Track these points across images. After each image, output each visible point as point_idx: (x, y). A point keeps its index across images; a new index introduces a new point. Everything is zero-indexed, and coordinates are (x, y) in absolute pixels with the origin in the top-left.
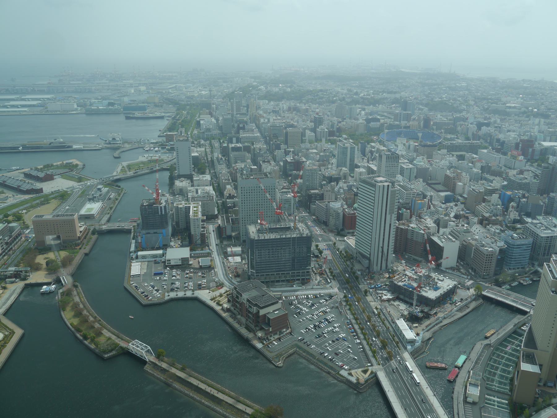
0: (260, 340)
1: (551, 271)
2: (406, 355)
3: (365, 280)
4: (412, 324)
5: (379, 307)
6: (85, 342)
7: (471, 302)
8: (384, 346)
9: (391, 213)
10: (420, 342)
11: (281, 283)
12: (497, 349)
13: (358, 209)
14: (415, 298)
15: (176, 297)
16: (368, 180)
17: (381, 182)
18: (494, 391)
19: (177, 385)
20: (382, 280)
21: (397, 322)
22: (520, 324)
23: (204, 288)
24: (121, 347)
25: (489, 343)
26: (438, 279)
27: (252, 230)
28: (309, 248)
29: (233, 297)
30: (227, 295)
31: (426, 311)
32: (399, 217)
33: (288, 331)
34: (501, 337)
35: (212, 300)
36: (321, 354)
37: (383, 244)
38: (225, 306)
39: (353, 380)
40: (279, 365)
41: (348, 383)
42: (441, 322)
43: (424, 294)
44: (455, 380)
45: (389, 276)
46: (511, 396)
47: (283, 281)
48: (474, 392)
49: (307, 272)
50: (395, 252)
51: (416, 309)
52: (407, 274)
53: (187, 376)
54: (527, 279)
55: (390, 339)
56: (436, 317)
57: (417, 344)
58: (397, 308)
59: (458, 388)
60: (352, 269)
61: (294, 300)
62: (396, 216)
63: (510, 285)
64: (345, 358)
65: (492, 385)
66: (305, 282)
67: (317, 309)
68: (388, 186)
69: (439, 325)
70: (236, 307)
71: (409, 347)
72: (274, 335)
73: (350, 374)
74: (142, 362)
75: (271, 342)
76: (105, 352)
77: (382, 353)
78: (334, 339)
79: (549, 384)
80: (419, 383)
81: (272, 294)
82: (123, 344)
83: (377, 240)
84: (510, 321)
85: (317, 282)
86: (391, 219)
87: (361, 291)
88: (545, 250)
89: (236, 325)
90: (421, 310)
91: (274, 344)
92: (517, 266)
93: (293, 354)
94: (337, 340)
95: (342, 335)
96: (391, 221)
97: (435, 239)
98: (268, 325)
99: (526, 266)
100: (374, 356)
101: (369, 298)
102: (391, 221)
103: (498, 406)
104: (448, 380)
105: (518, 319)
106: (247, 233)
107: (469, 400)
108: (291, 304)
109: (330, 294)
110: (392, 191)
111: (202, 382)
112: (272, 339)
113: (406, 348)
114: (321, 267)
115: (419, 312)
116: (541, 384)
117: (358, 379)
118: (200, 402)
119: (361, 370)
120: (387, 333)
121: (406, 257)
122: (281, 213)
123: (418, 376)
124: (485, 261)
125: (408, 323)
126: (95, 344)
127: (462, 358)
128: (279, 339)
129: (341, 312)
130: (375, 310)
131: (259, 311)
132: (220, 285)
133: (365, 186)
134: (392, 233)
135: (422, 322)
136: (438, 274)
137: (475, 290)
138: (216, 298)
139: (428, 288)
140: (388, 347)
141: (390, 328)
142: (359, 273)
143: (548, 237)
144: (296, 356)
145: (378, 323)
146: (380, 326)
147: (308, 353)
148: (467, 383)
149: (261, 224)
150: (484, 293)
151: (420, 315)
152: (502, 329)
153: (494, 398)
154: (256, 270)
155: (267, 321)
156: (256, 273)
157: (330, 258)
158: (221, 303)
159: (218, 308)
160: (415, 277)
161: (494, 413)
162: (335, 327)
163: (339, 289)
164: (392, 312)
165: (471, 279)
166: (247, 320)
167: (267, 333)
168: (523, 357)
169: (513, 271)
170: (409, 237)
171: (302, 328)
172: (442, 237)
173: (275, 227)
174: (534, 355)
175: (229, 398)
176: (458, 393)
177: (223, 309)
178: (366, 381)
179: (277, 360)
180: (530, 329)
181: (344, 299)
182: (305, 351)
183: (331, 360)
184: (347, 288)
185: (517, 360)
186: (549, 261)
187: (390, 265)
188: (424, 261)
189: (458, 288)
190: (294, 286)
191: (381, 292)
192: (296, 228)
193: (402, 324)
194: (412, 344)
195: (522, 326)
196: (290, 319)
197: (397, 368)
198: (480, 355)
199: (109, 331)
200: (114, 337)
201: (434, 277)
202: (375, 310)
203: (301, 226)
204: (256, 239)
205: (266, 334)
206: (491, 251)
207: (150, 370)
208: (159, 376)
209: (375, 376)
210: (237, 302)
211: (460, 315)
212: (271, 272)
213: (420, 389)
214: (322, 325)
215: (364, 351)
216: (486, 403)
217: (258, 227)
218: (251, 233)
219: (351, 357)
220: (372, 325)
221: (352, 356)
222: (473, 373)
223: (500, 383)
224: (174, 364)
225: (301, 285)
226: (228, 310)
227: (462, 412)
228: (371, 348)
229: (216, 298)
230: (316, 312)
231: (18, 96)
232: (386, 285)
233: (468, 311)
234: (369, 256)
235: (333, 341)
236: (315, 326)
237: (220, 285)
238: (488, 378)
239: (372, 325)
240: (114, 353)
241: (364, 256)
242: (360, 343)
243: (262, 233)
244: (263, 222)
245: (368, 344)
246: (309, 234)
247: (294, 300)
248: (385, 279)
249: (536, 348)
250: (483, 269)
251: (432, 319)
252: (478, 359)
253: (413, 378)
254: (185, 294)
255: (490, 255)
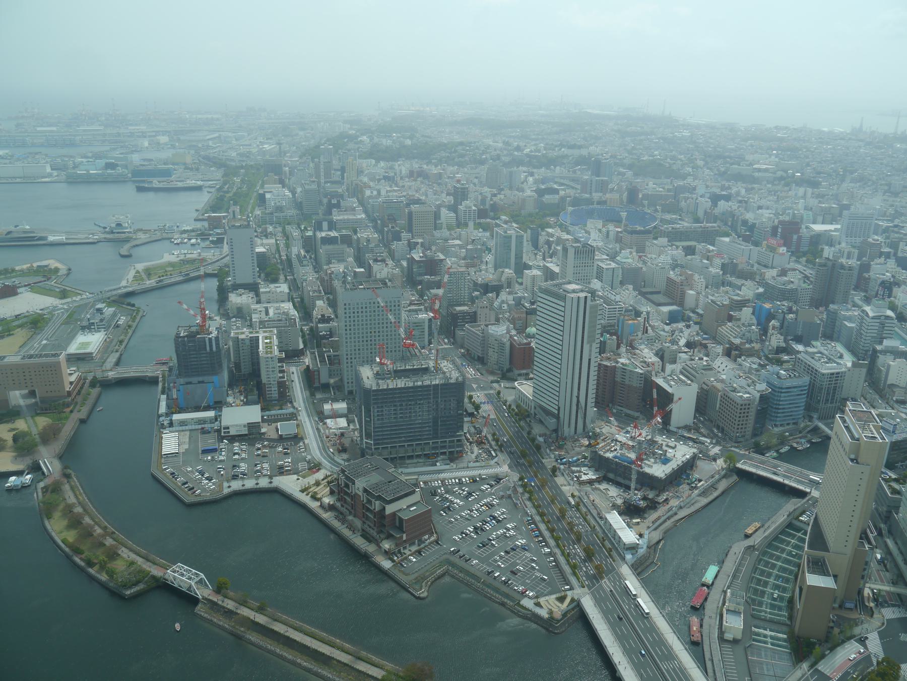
0: (388, 554)
1: (847, 428)
2: (625, 570)
3: (551, 450)
4: (631, 519)
5: (576, 493)
6: (90, 570)
7: (719, 480)
8: (589, 555)
9: (590, 342)
10: (645, 547)
11: (415, 461)
12: (764, 553)
13: (537, 336)
14: (634, 477)
15: (241, 488)
16: (552, 288)
17: (574, 291)
18: (765, 620)
19: (253, 637)
20: (577, 449)
21: (608, 516)
22: (797, 513)
23: (289, 473)
24: (154, 577)
25: (752, 544)
26: (667, 446)
27: (367, 374)
28: (460, 402)
29: (338, 485)
30: (329, 483)
31: (650, 496)
32: (602, 349)
33: (432, 539)
34: (770, 534)
35: (302, 491)
36: (489, 573)
37: (579, 394)
38: (327, 500)
39: (544, 613)
40: (422, 595)
41: (536, 618)
42: (676, 514)
43: (647, 470)
44: (703, 606)
45: (590, 444)
46: (791, 627)
47: (418, 456)
48: (735, 624)
49: (459, 441)
50: (597, 404)
51: (635, 495)
52: (618, 439)
53: (270, 620)
54: (803, 441)
55: (598, 545)
56: (667, 507)
57: (641, 551)
58: (604, 493)
59: (711, 620)
60: (529, 433)
61: (439, 487)
62: (598, 345)
63: (777, 451)
64: (528, 579)
65: (760, 611)
66: (454, 457)
67: (477, 501)
68: (586, 297)
69: (672, 520)
70: (345, 501)
71: (629, 557)
72: (410, 545)
73: (538, 605)
74: (188, 599)
75: (406, 558)
76: (126, 586)
77: (587, 568)
78: (508, 549)
79: (848, 605)
80: (647, 614)
81: (403, 478)
82: (156, 572)
83: (569, 386)
84: (780, 507)
85: (473, 456)
86: (590, 351)
87: (546, 469)
88: (828, 394)
89: (346, 532)
90: (644, 495)
91: (411, 561)
92: (796, 420)
93: (442, 576)
94: (513, 549)
95: (521, 542)
96: (590, 355)
97: (660, 381)
98: (400, 529)
99: (800, 421)
100: (575, 574)
101: (560, 480)
102: (590, 355)
103: (772, 644)
104: (692, 607)
105: (792, 504)
106: (358, 379)
107: (729, 636)
108: (434, 494)
109: (497, 475)
110: (591, 307)
111: (295, 629)
112: (407, 552)
113: (623, 559)
114: (480, 432)
115: (639, 500)
116: (836, 605)
117: (551, 612)
118: (294, 663)
119: (554, 596)
120: (592, 535)
121: (615, 411)
122: (413, 345)
123: (645, 603)
124: (738, 415)
125: (625, 518)
126: (107, 573)
127: (712, 571)
128: (419, 552)
129: (515, 505)
130: (571, 499)
131: (384, 508)
132: (315, 467)
133: (549, 298)
134: (592, 373)
135: (646, 515)
136: (667, 437)
137: (725, 462)
138: (309, 487)
139: (652, 460)
140: (596, 558)
141: (597, 527)
142: (541, 439)
143: (832, 374)
144: (447, 579)
145: (577, 520)
146: (581, 524)
147: (467, 573)
148: (722, 610)
149: (381, 364)
150: (739, 465)
151: (642, 504)
152: (770, 522)
153: (765, 632)
154: (375, 440)
155: (397, 524)
156: (375, 445)
157: (492, 416)
158: (319, 496)
159: (314, 505)
160: (631, 443)
161: (766, 655)
162: (508, 530)
163: (510, 467)
164: (597, 501)
165: (718, 443)
166: (364, 523)
167: (400, 543)
168: (808, 564)
169: (781, 429)
170: (618, 379)
171: (456, 532)
172: (669, 378)
173: (403, 368)
174: (824, 560)
175: (343, 654)
176: (710, 626)
177: (322, 506)
178: (564, 615)
179: (417, 587)
180: (816, 519)
181: (520, 483)
182: (462, 570)
183: (505, 583)
184: (524, 464)
185: (796, 569)
186: (843, 412)
187: (590, 426)
188: (641, 417)
189: (699, 458)
190: (438, 464)
191: (578, 469)
192: (437, 369)
193: (616, 520)
194: (634, 551)
195: (801, 515)
196: (435, 518)
197: (611, 591)
198: (740, 564)
199: (131, 550)
200: (140, 561)
201: (660, 442)
202: (571, 499)
203: (445, 365)
204: (374, 388)
205: (397, 545)
206: (748, 399)
207: (206, 613)
208: (221, 623)
209: (577, 606)
210: (346, 493)
211: (704, 501)
212: (400, 442)
213: (649, 622)
214: (487, 527)
215: (558, 566)
216: (754, 640)
217: (376, 369)
218: (365, 380)
219: (537, 577)
220: (569, 524)
221: (538, 574)
222: (732, 594)
223: (773, 607)
224: (246, 602)
225: (448, 462)
226: (331, 508)
227: (717, 657)
228: (568, 561)
229: (309, 487)
230: (477, 506)
231: (7, 151)
232: (585, 458)
233: (715, 494)
234: (556, 412)
235: (507, 552)
236: (476, 528)
237: (315, 467)
238: (753, 600)
239: (569, 524)
240: (141, 587)
241: (548, 413)
242: (550, 554)
243: (383, 379)
244: (385, 361)
245: (563, 554)
246: (460, 379)
247: (439, 487)
248: (583, 448)
249: (827, 550)
250: (736, 427)
251: (661, 511)
252: (737, 571)
253: (638, 606)
254: (257, 484)
255: (747, 405)
